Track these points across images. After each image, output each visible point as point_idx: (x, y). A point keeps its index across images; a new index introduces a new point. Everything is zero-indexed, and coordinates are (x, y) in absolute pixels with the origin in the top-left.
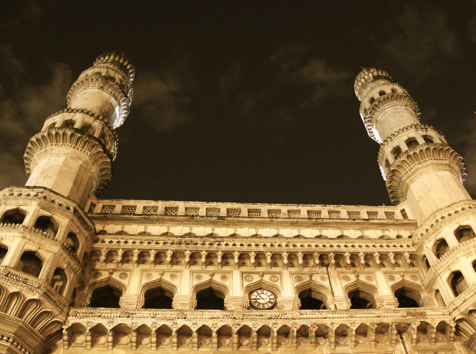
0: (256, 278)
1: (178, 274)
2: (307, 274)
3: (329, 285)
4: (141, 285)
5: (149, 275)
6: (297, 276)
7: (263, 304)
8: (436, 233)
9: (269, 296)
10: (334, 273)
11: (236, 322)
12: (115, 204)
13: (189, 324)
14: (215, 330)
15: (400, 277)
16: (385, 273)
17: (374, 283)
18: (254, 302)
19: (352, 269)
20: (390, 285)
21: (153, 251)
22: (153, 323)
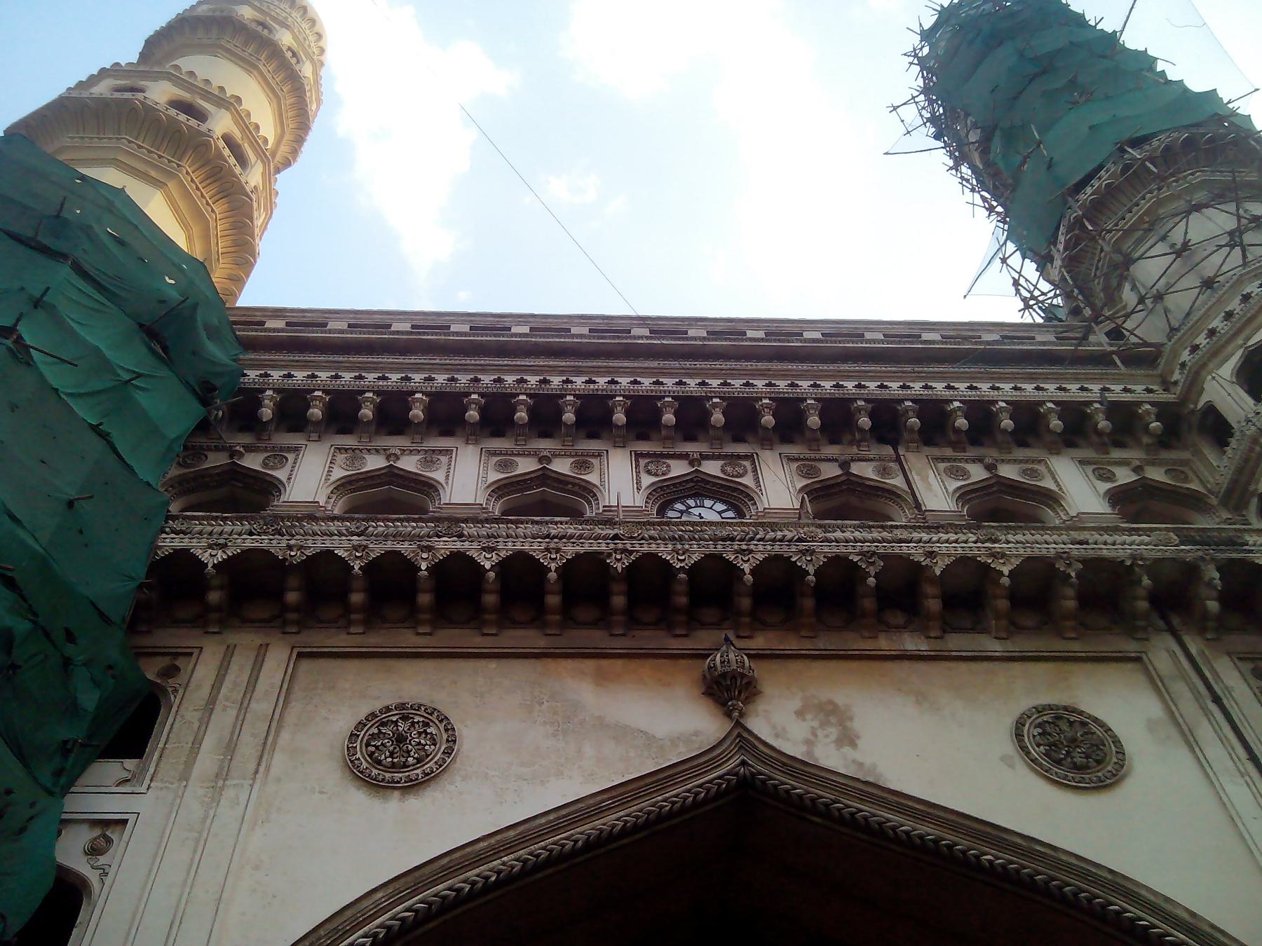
0: (679, 469)
2: (836, 460)
3: (905, 487)
8: (1247, 332)
11: (620, 546)
14: (553, 566)
16: (1083, 462)
17: (1048, 484)
19: (972, 452)
20: (1102, 491)
22: (356, 548)
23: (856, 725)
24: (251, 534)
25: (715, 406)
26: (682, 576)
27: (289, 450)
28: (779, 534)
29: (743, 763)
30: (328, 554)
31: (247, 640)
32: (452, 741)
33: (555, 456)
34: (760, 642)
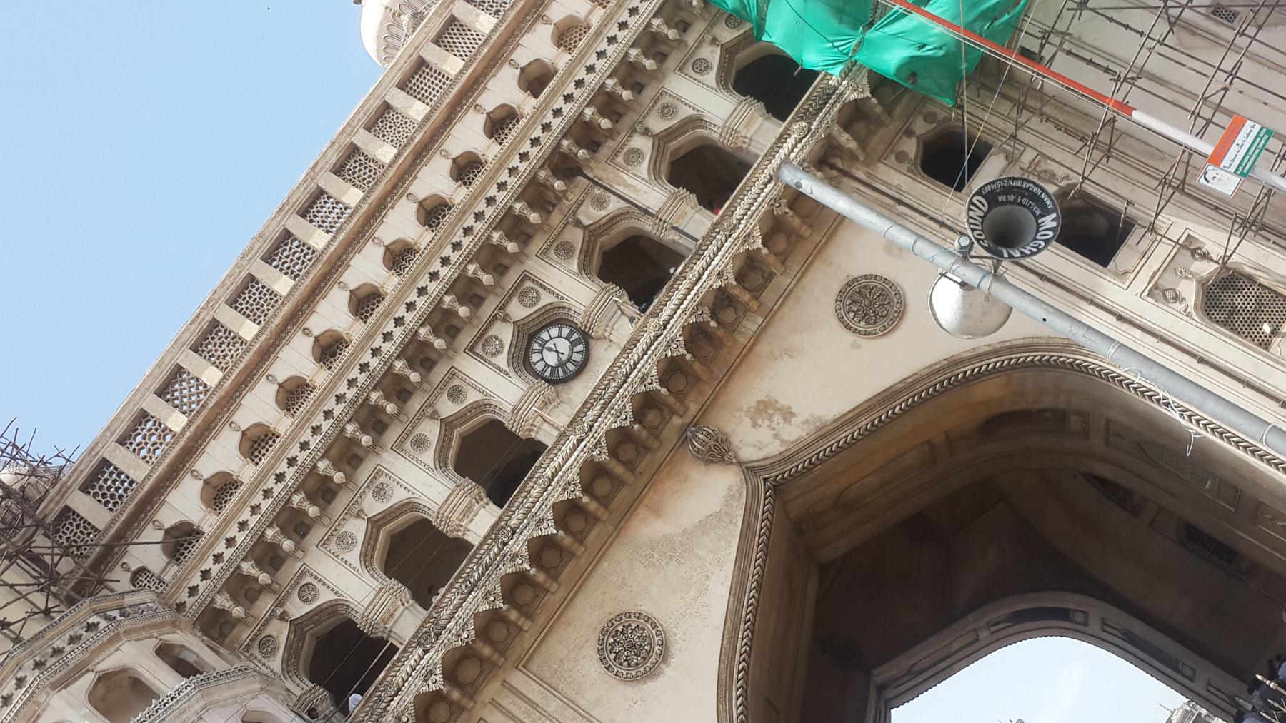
0: (505, 333)
1: (382, 479)
3: (623, 204)
4: (358, 566)
5: (345, 540)
6: (557, 249)
7: (569, 360)
9: (560, 336)
10: (604, 170)
12: (62, 505)
13: (532, 532)
15: (712, 47)
17: (685, 112)
18: (551, 374)
20: (714, 84)
21: (296, 499)
22: (485, 597)
23: (782, 402)
24: (426, 652)
25: (475, 272)
26: (636, 426)
27: (300, 577)
28: (641, 346)
29: (765, 480)
30: (476, 615)
31: (492, 689)
32: (648, 619)
33: (431, 405)
34: (693, 408)
